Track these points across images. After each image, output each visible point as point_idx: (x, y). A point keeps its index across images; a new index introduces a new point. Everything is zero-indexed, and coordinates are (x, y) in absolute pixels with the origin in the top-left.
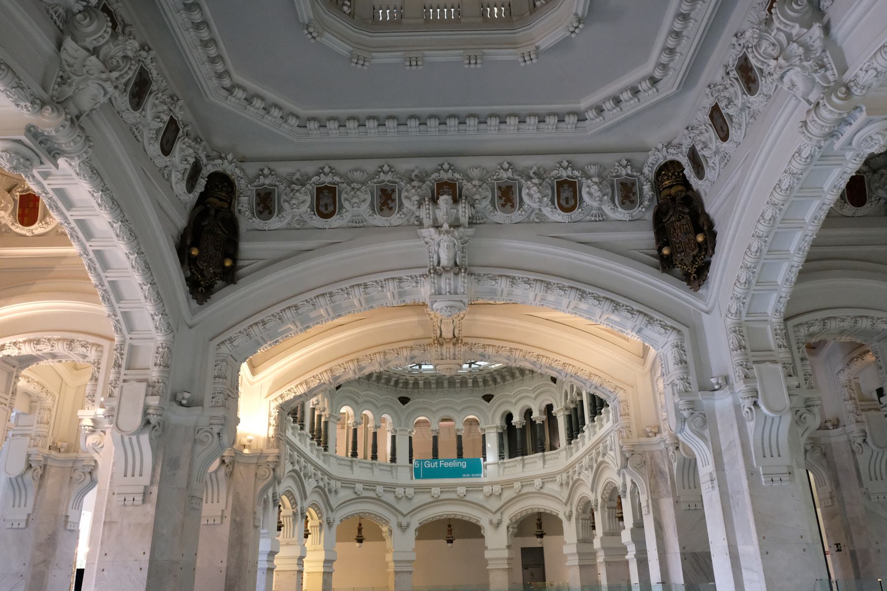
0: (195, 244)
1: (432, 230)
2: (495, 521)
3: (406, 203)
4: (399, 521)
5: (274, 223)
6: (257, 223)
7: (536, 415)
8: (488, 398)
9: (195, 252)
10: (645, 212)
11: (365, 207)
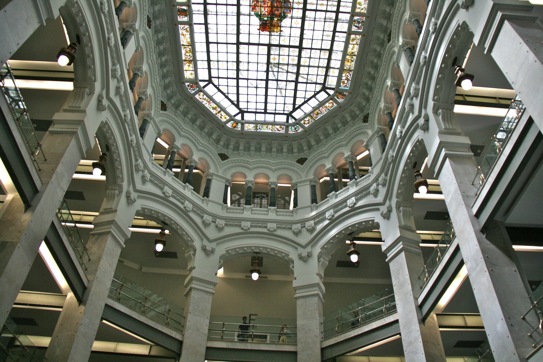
2: (305, 254)
4: (203, 243)
8: (301, 161)
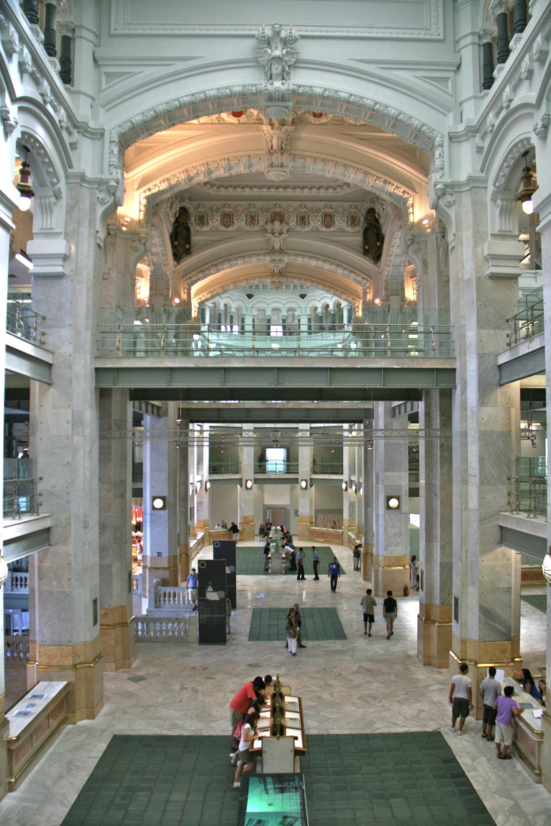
0: (176, 240)
1: (271, 235)
3: (261, 222)
5: (206, 229)
6: (198, 228)
7: (331, 307)
9: (176, 243)
10: (360, 229)
11: (243, 223)
